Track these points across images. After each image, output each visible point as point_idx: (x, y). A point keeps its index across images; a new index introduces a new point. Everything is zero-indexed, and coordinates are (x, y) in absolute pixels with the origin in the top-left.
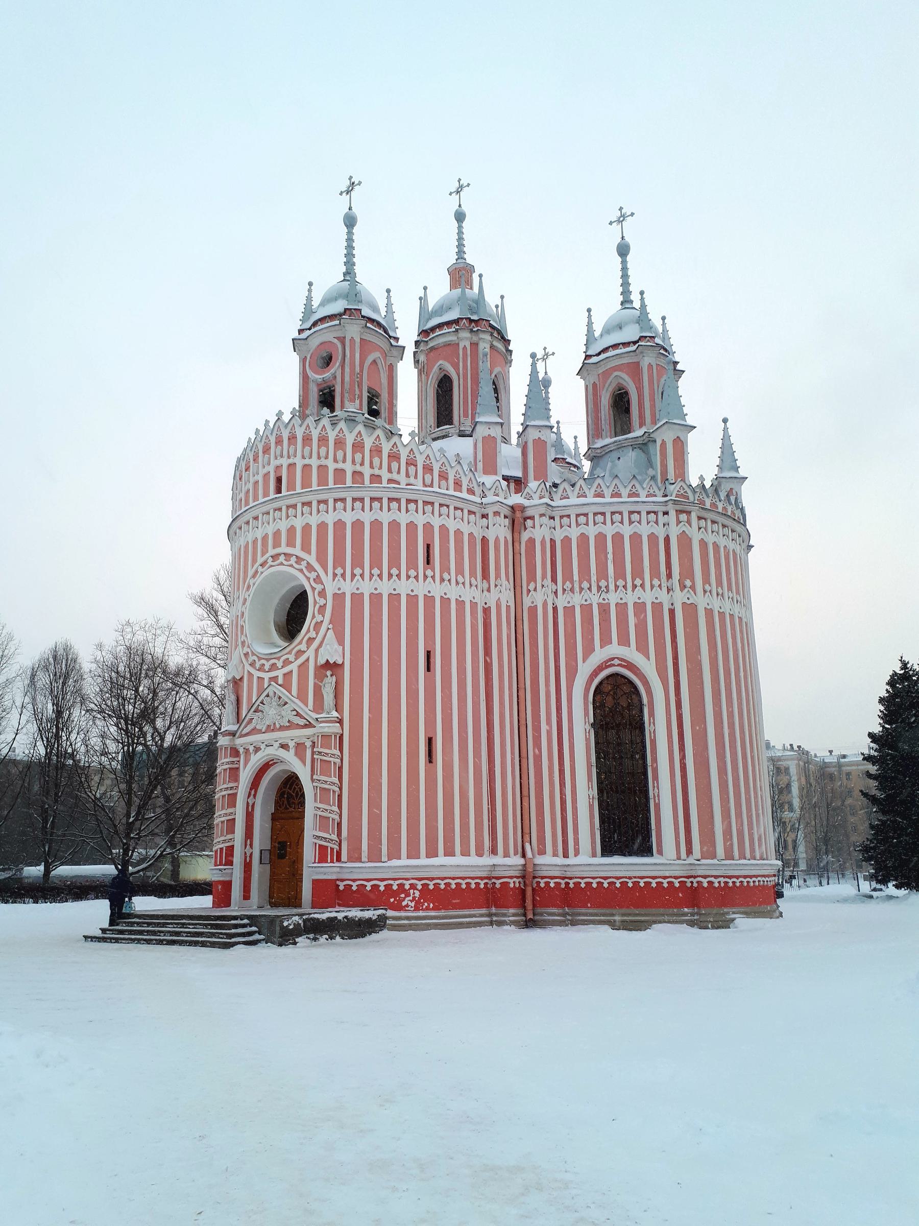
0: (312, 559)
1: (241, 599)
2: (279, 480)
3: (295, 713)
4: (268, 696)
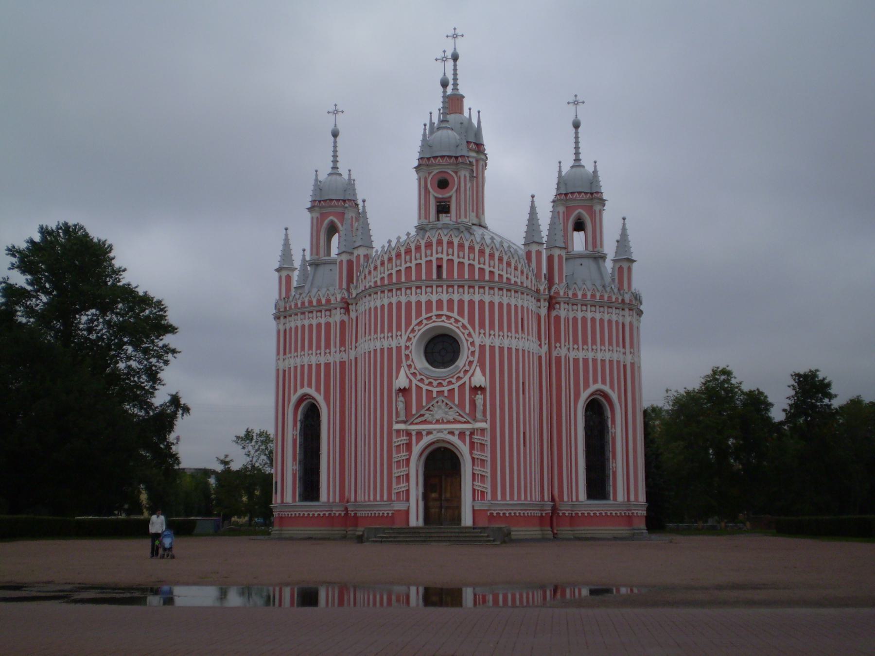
0: (465, 321)
1: (405, 338)
2: (439, 267)
3: (458, 414)
4: (437, 402)
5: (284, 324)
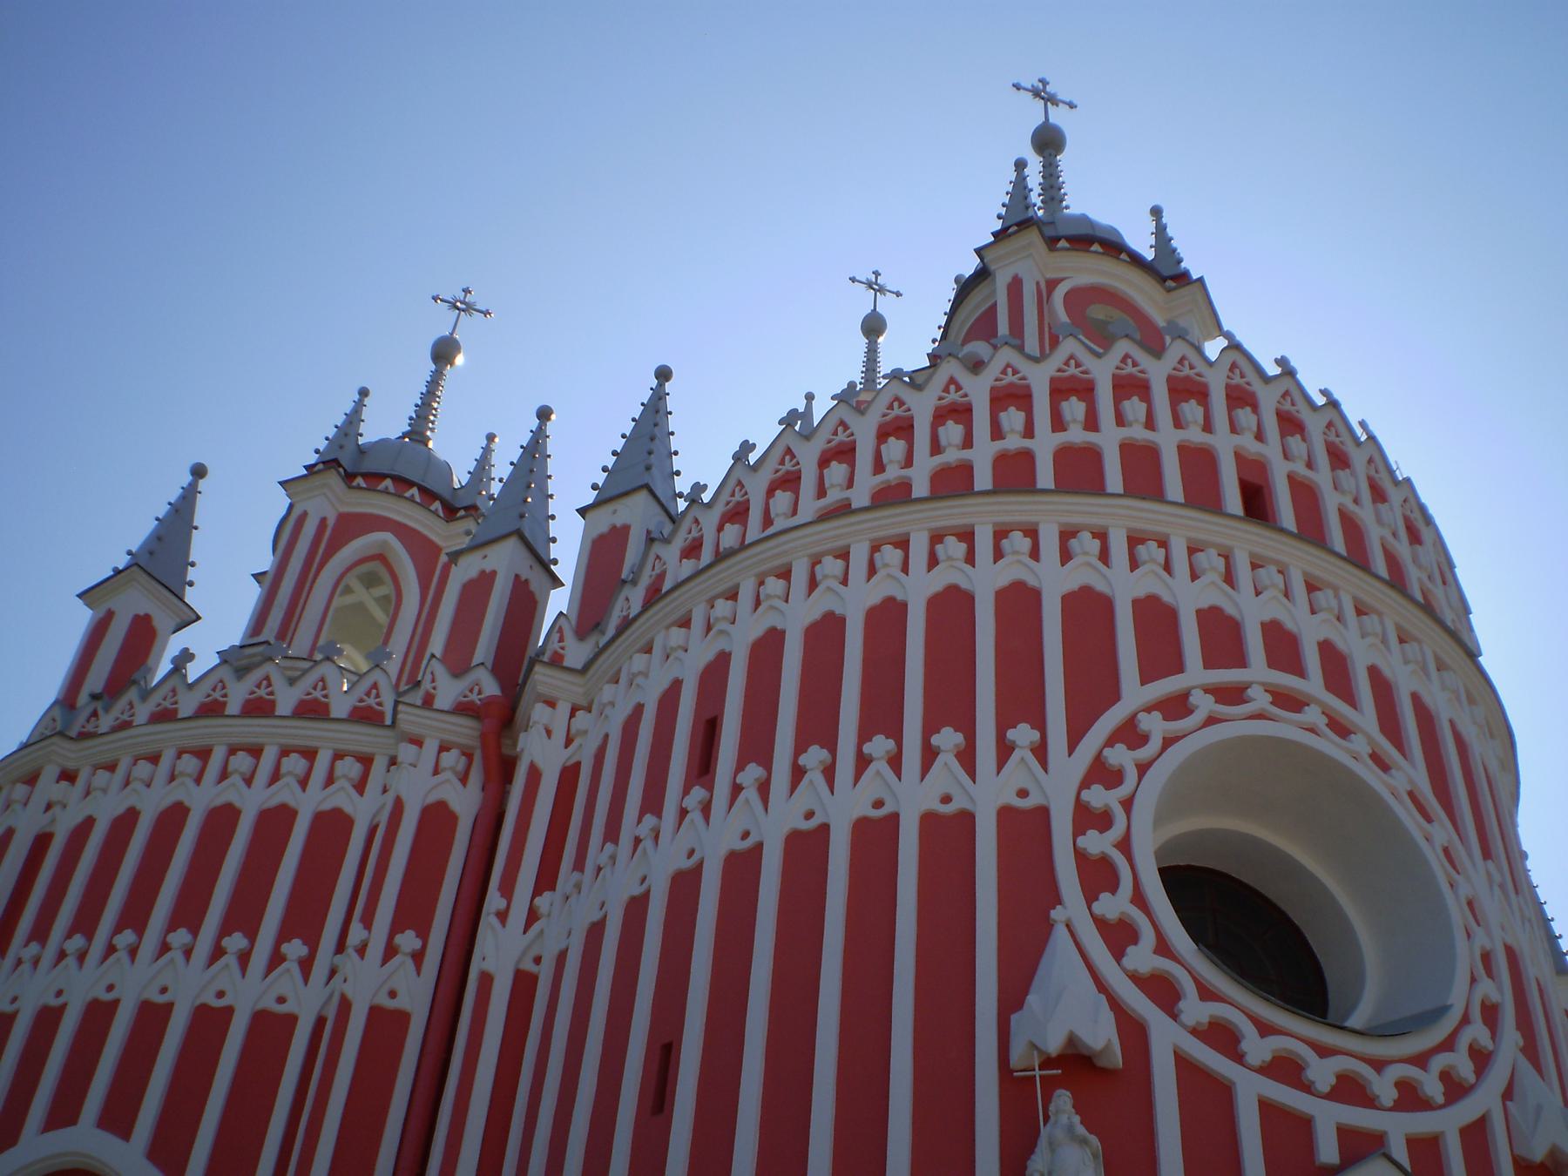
5: (49, 807)
